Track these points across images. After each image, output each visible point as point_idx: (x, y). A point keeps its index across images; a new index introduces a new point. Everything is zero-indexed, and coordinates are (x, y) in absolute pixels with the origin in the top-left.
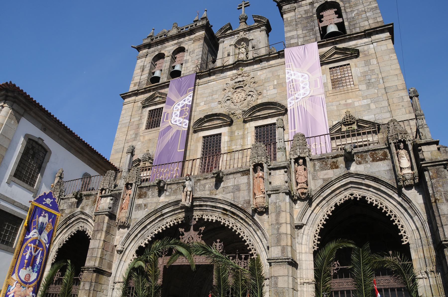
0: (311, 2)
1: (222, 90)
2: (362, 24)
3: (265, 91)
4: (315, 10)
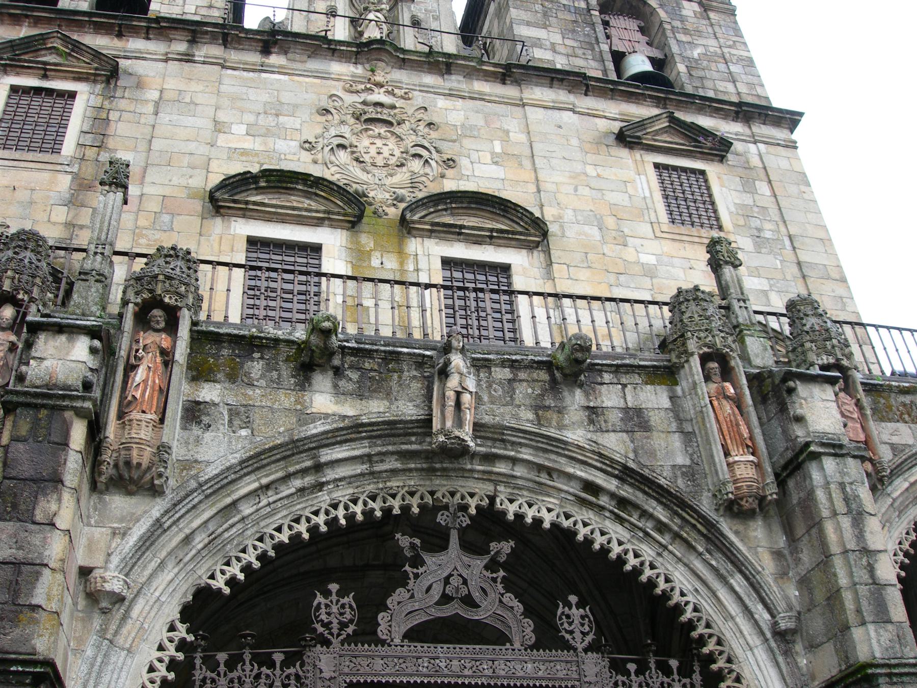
1: (314, 111)
3: (464, 162)
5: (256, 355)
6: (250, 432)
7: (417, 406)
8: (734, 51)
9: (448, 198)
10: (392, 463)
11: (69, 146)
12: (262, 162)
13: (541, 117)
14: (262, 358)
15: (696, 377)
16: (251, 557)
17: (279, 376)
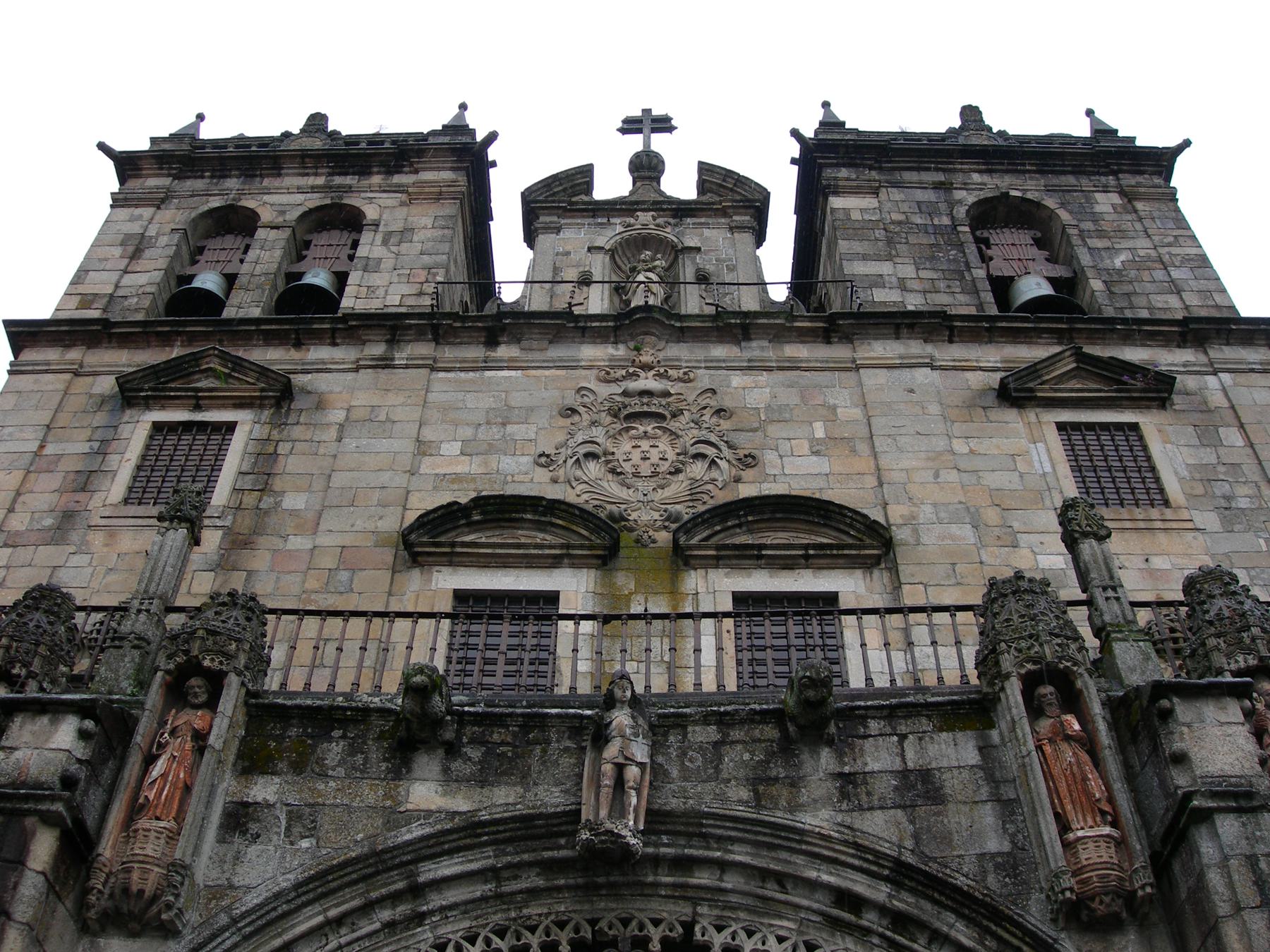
0: (942, 183)
2: (1159, 301)
3: (770, 457)
4: (961, 212)
5: (337, 733)
6: (314, 842)
7: (566, 792)
8: (1174, 250)
9: (740, 509)
10: (533, 880)
12: (481, 488)
14: (344, 737)
15: (1014, 711)
17: (366, 760)
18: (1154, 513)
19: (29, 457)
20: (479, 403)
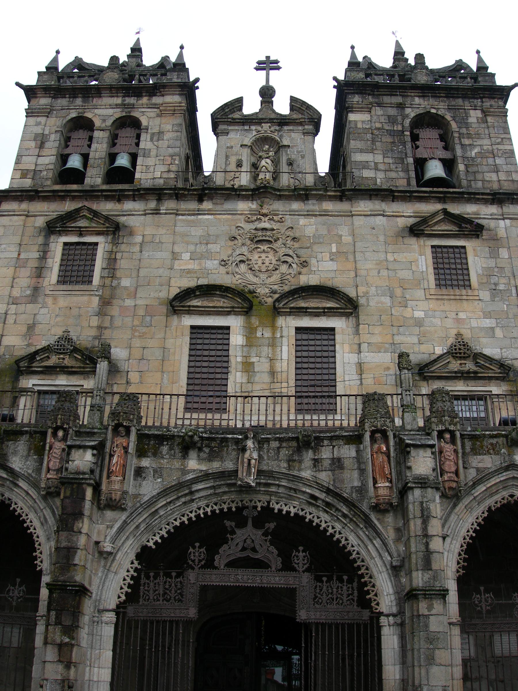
0: (401, 104)
3: (313, 261)
4: (407, 122)
5: (165, 443)
8: (500, 147)
11: (96, 280)
13: (362, 223)
14: (167, 444)
16: (164, 533)
17: (175, 452)
18: (464, 292)
19: (15, 260)
20: (197, 232)
